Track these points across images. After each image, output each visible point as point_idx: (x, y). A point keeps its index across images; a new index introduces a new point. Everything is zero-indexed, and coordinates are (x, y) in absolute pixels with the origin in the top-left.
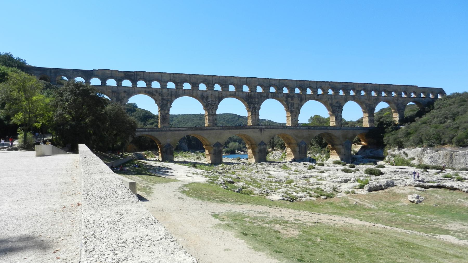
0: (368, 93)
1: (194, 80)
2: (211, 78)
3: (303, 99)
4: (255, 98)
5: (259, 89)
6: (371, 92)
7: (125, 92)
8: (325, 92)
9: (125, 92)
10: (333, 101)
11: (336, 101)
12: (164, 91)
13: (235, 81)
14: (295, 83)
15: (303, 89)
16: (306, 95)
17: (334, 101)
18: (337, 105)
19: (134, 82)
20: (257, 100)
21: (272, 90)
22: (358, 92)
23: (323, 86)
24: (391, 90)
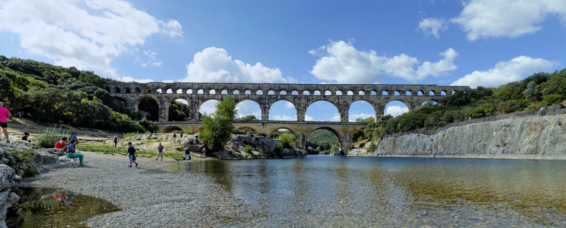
0: (379, 93)
1: (216, 87)
2: (230, 85)
3: (310, 100)
4: (265, 99)
5: (271, 93)
6: (381, 91)
7: (166, 97)
8: (334, 94)
9: (166, 97)
10: (340, 101)
11: (343, 101)
12: (194, 96)
13: (250, 87)
14: (304, 86)
15: (312, 92)
16: (312, 96)
17: (341, 101)
18: (344, 104)
19: (174, 90)
20: (267, 101)
21: (283, 93)
22: (367, 92)
23: (330, 88)
24: (405, 90)
